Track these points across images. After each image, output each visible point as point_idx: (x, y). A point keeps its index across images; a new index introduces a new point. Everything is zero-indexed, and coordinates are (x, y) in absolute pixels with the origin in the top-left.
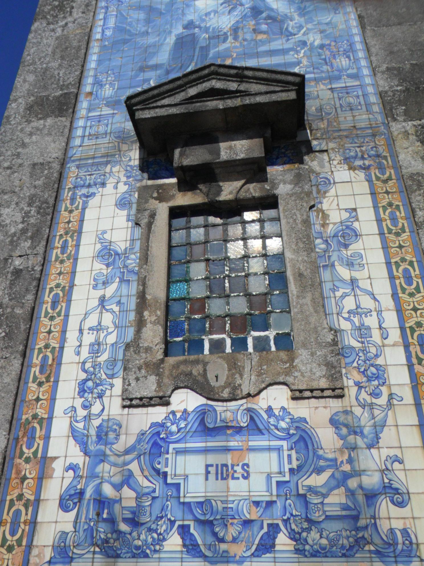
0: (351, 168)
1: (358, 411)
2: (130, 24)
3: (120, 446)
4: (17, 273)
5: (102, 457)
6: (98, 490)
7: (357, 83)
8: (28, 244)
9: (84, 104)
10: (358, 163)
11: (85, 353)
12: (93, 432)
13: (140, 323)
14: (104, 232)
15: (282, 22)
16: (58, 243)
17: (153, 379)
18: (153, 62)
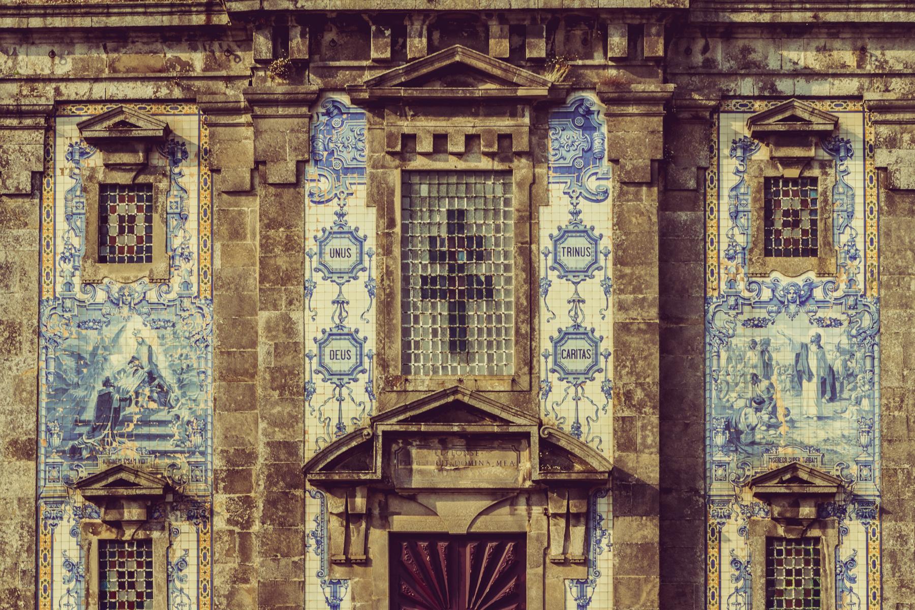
4: (24, 572)
7: (203, 460)
9: (43, 451)
15: (167, 392)
18: (83, 418)
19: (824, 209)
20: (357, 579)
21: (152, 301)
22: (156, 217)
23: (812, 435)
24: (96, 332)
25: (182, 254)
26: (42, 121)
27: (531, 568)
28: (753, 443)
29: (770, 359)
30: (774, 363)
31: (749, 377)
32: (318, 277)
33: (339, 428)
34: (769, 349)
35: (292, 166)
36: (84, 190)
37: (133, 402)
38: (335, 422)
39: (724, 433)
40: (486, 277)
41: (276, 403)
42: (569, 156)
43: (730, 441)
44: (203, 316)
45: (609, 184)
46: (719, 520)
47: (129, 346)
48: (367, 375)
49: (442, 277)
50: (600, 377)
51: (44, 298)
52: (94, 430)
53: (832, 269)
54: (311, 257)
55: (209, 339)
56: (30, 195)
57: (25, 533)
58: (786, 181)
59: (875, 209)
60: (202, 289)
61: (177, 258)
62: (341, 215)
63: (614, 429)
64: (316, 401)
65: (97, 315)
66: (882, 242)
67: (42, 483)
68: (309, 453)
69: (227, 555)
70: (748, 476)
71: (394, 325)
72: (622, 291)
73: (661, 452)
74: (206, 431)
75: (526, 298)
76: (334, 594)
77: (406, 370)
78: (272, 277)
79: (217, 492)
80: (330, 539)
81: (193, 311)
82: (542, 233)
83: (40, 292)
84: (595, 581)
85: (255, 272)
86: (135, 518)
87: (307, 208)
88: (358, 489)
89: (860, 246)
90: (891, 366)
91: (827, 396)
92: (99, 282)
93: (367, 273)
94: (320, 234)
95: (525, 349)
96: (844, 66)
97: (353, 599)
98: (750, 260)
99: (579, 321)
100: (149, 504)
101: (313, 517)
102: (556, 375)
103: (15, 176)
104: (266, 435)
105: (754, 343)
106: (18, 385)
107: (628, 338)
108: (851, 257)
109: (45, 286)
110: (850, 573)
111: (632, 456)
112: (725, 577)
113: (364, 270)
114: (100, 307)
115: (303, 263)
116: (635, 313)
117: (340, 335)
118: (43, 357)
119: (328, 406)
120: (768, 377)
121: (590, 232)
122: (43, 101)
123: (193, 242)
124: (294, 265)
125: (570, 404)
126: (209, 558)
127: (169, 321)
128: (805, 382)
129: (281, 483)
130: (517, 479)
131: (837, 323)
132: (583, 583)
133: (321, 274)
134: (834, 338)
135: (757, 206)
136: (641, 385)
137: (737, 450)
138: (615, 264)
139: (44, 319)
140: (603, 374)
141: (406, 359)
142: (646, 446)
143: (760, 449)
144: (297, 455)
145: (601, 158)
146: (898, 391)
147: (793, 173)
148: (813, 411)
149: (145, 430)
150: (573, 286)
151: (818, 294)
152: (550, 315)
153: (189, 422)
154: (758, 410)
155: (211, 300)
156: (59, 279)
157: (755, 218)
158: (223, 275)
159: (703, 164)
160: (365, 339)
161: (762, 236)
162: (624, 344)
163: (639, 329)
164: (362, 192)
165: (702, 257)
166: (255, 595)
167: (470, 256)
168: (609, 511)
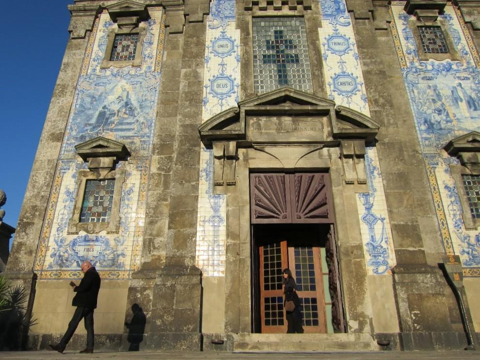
0: (137, 170)
1: (121, 237)
2: (85, 104)
3: (66, 244)
4: (43, 197)
5: (61, 246)
6: (60, 254)
7: (148, 139)
8: (46, 188)
9: (66, 138)
10: (140, 169)
11: (59, 220)
12: (59, 240)
13: (74, 213)
14: (67, 186)
15: (134, 110)
16: (54, 188)
17: (75, 228)
18: (89, 123)
20: (229, 194)
22: (138, 44)
24: (103, 87)
25: (149, 56)
26: (95, 13)
27: (335, 187)
28: (441, 129)
29: (439, 93)
30: (441, 94)
31: (431, 100)
34: (437, 88)
35: (201, 15)
36: (108, 36)
37: (116, 115)
39: (424, 125)
40: (295, 55)
44: (156, 79)
45: (350, 20)
46: (432, 166)
47: (118, 91)
48: (236, 94)
49: (273, 56)
50: (359, 94)
52: (94, 128)
55: (158, 88)
57: (48, 177)
58: (426, 27)
59: (470, 37)
65: (105, 80)
67: (63, 153)
70: (442, 144)
72: (364, 58)
75: (317, 60)
78: (189, 56)
79: (154, 154)
82: (320, 37)
83: (80, 73)
84: (374, 194)
86: (106, 166)
87: (207, 31)
89: (468, 50)
91: (473, 108)
92: (109, 68)
94: (213, 40)
97: (227, 205)
100: (115, 158)
102: (336, 93)
106: (60, 110)
107: (371, 77)
108: (465, 54)
113: (234, 52)
115: (204, 50)
117: (222, 78)
119: (214, 108)
120: (440, 100)
123: (155, 51)
124: (200, 51)
126: (146, 188)
127: (139, 81)
128: (459, 103)
130: (323, 137)
132: (367, 195)
133: (213, 54)
134: (467, 84)
135: (417, 35)
137: (433, 132)
139: (79, 83)
143: (446, 132)
145: (344, 12)
149: (120, 127)
150: (340, 57)
151: (454, 67)
152: (329, 68)
153: (143, 123)
154: (439, 114)
155: (160, 73)
157: (416, 39)
159: (389, 20)
160: (235, 79)
161: (422, 45)
162: (369, 79)
164: (233, 24)
165: (396, 53)
167: (286, 47)
168: (375, 156)
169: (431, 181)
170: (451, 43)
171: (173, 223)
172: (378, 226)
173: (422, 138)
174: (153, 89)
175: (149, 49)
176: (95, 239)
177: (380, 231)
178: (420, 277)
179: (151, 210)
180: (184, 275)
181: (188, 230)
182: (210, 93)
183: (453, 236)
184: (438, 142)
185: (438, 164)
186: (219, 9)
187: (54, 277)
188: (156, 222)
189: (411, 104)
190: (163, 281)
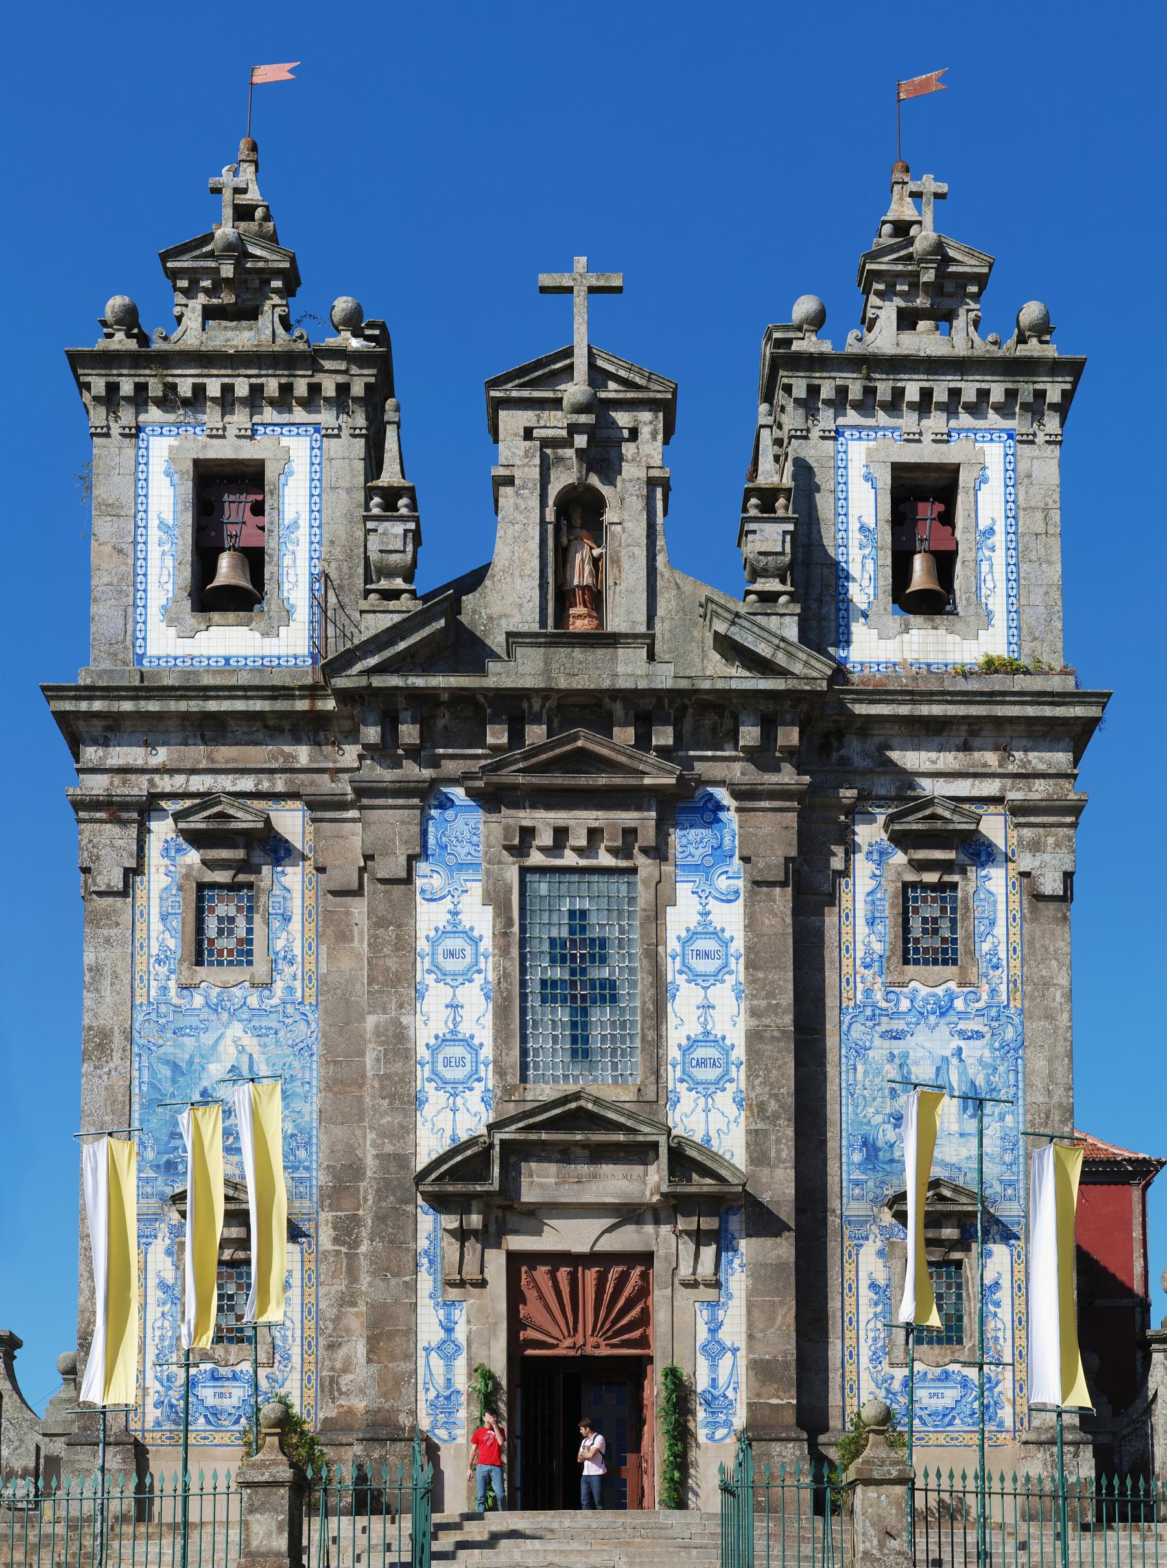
5: (170, 1388)
6: (169, 1401)
19: (965, 917)
21: (253, 1007)
22: (257, 918)
23: (954, 1153)
24: (193, 1039)
28: (892, 1161)
29: (909, 1073)
31: (887, 1092)
32: (430, 979)
33: (453, 1140)
34: (908, 1062)
36: (180, 888)
38: (449, 1133)
39: (861, 1151)
41: (386, 1113)
42: (697, 853)
43: (868, 1159)
44: (308, 1022)
49: (563, 981)
51: (138, 1002)
53: (974, 979)
54: (423, 958)
55: (314, 1047)
56: (124, 893)
58: (925, 886)
59: (1018, 916)
60: (307, 994)
61: (280, 961)
62: (455, 914)
63: (747, 1143)
64: (428, 1110)
65: (195, 1021)
66: (1025, 952)
68: (422, 1162)
69: (333, 1277)
71: (512, 1030)
72: (754, 997)
73: (796, 1168)
74: (311, 1145)
76: (448, 1317)
77: (524, 1079)
80: (443, 1257)
81: (298, 1017)
85: (363, 976)
88: (474, 1203)
89: (1003, 955)
90: (1037, 1082)
92: (197, 987)
93: (482, 975)
95: (651, 1057)
96: (985, 765)
97: (469, 1322)
98: (888, 968)
99: (709, 1028)
101: (425, 1235)
102: (685, 1085)
103: (105, 872)
104: (374, 1145)
105: (892, 1055)
109: (138, 990)
110: (995, 1297)
111: (766, 1171)
112: (863, 1301)
113: (479, 972)
114: (197, 1012)
116: (769, 1020)
117: (454, 1040)
118: (136, 1066)
119: (440, 1117)
121: (720, 934)
122: (136, 792)
125: (700, 1116)
126: (314, 1280)
127: (271, 1028)
129: (391, 1198)
131: (979, 1035)
133: (433, 976)
134: (974, 1051)
136: (775, 1095)
138: (746, 968)
139: (137, 1026)
140: (735, 1084)
141: (524, 1067)
142: (779, 1160)
144: (408, 1168)
145: (731, 856)
146: (1043, 1107)
147: (931, 877)
148: (954, 1128)
151: (959, 1004)
155: (317, 1006)
156: (153, 983)
158: (329, 979)
160: (481, 1045)
162: (757, 1052)
163: (773, 1037)
166: (364, 1319)
169: (846, 1273)
170: (970, 936)
171: (375, 1353)
172: (726, 1362)
173: (850, 1180)
174: (302, 1050)
175: (284, 933)
176: (230, 1375)
177: (728, 1372)
178: (776, 1447)
179: (328, 1323)
180: (400, 1440)
181: (404, 1366)
182: (430, 1080)
183: (864, 1376)
184: (878, 1191)
185: (867, 1239)
186: (444, 839)
187: (168, 1442)
188: (340, 1344)
189: (844, 1102)
190: (365, 1450)
